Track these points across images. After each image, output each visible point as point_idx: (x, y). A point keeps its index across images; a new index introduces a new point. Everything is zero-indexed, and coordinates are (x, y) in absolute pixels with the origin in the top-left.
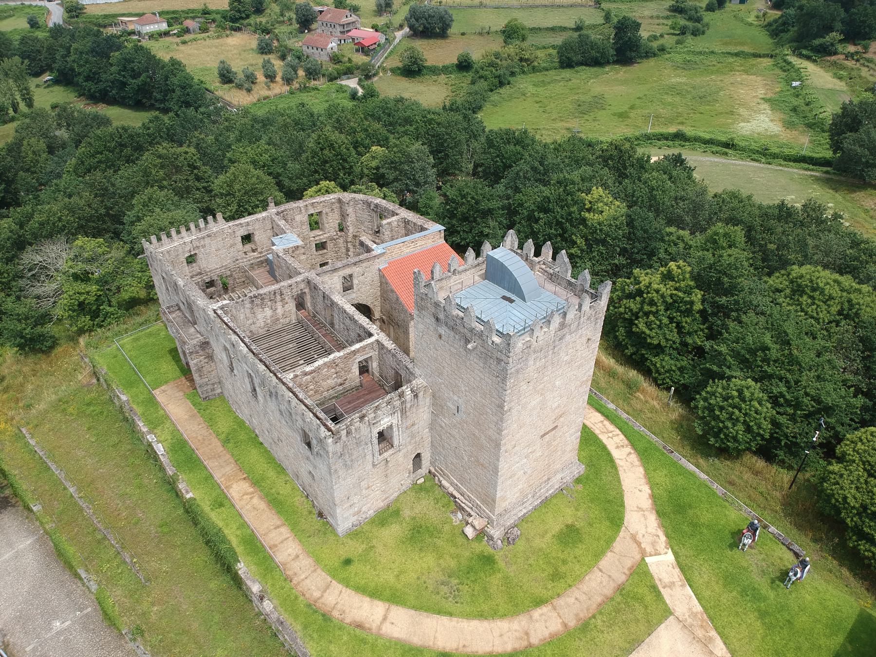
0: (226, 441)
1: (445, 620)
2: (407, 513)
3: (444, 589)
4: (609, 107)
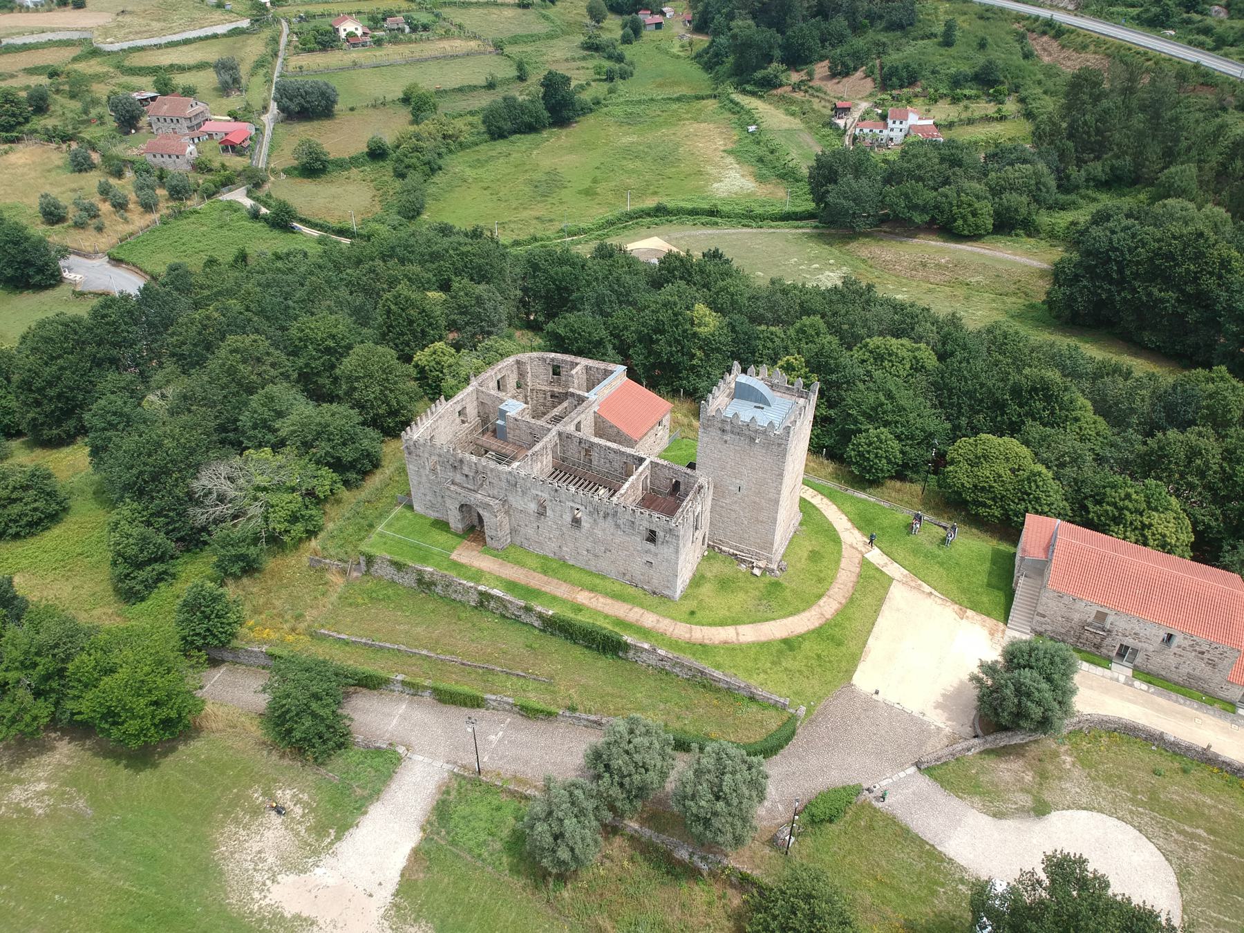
0: (545, 572)
2: (709, 575)
4: (569, 184)
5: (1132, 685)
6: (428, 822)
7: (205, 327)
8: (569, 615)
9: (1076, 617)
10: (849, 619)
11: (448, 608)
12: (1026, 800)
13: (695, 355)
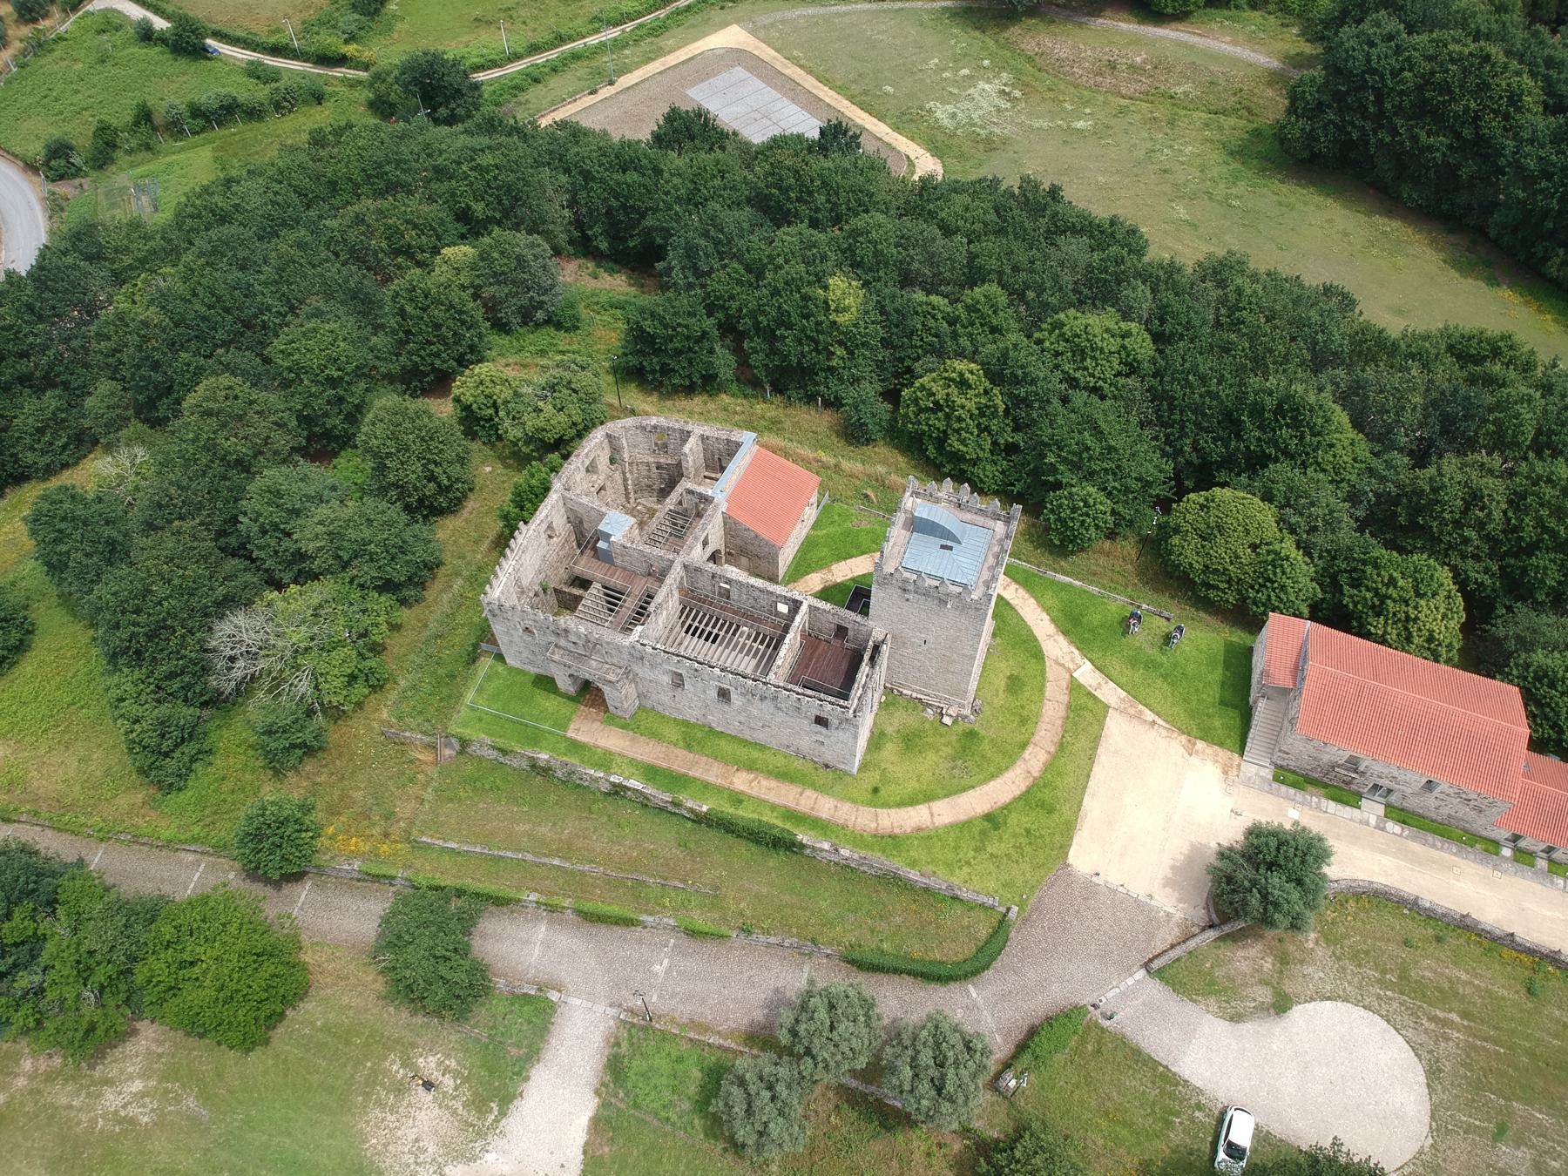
0: (689, 747)
1: (971, 792)
2: (890, 730)
3: (957, 772)
5: (1383, 829)
6: (603, 1084)
7: (145, 339)
8: (729, 810)
9: (1326, 758)
10: (1059, 774)
11: (573, 797)
12: (1264, 995)
13: (833, 354)
